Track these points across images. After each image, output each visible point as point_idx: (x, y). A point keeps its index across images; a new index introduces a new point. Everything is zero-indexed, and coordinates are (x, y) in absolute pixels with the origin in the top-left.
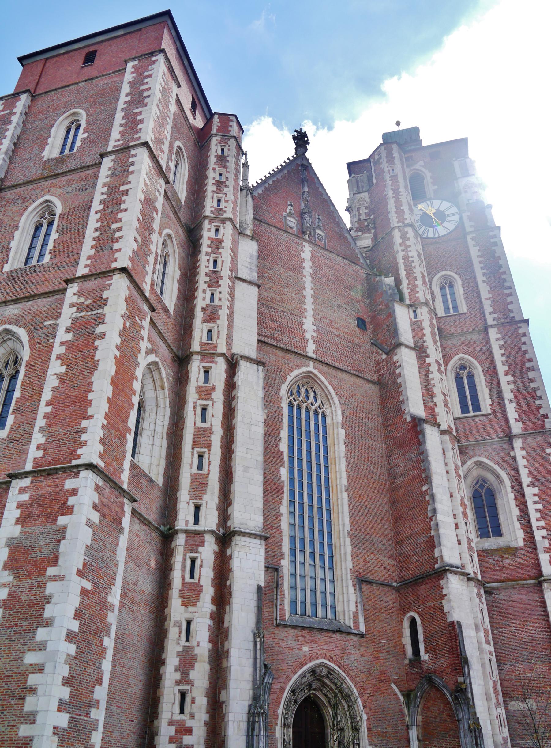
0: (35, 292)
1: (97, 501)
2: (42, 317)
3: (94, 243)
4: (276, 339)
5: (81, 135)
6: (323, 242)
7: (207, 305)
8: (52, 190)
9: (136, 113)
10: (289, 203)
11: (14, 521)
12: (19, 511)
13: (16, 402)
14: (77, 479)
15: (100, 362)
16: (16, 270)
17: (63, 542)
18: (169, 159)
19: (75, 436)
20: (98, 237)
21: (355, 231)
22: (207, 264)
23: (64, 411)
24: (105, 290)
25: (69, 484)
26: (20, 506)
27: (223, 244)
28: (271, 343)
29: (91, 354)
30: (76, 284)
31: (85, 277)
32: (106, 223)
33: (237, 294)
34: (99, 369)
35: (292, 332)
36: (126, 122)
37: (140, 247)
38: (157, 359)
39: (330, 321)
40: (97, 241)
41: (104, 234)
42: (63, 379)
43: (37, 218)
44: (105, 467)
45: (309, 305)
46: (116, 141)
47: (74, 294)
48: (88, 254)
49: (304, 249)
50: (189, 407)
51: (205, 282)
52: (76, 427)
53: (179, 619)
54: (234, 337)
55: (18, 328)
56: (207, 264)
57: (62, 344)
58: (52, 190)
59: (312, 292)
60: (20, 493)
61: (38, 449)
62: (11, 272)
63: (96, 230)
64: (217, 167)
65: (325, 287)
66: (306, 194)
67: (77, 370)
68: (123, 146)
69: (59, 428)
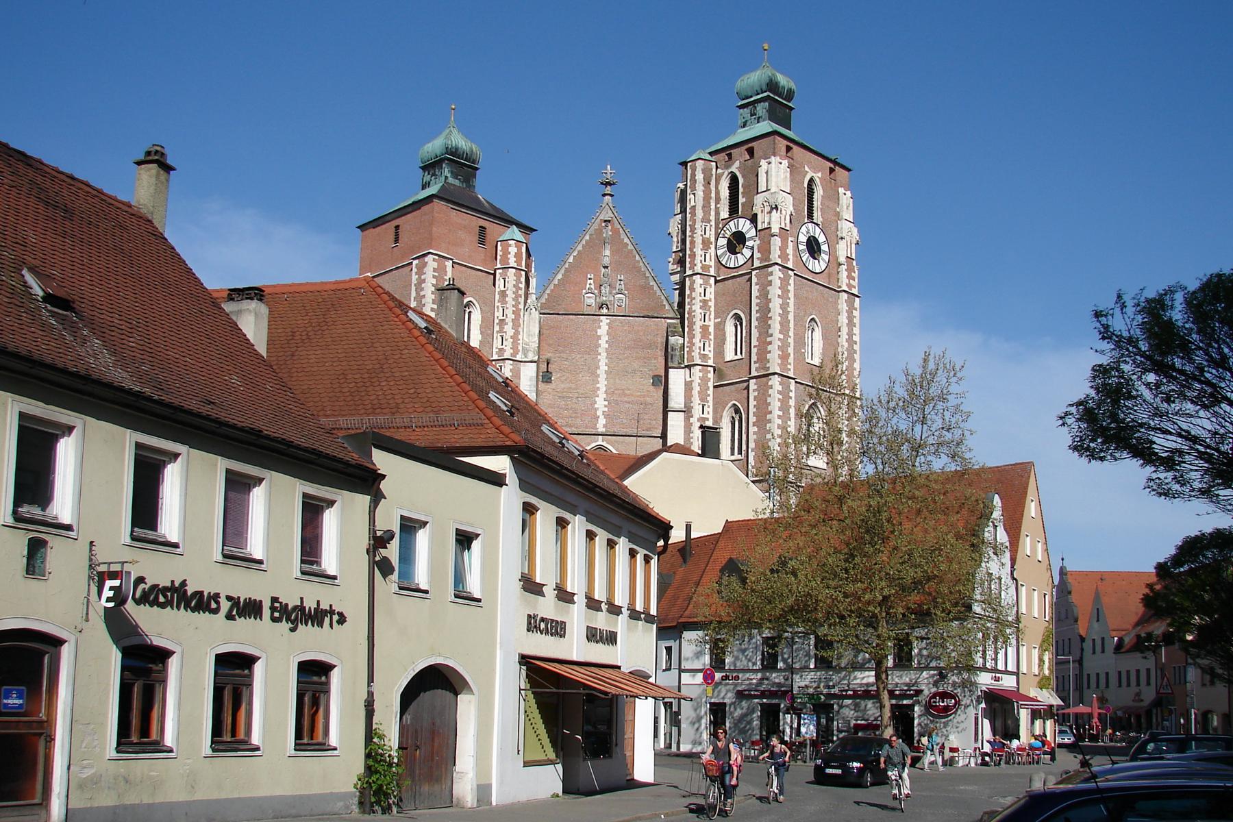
10: (589, 276)
21: (672, 264)
39: (623, 390)
45: (602, 384)
59: (606, 368)
64: (499, 304)
65: (620, 357)
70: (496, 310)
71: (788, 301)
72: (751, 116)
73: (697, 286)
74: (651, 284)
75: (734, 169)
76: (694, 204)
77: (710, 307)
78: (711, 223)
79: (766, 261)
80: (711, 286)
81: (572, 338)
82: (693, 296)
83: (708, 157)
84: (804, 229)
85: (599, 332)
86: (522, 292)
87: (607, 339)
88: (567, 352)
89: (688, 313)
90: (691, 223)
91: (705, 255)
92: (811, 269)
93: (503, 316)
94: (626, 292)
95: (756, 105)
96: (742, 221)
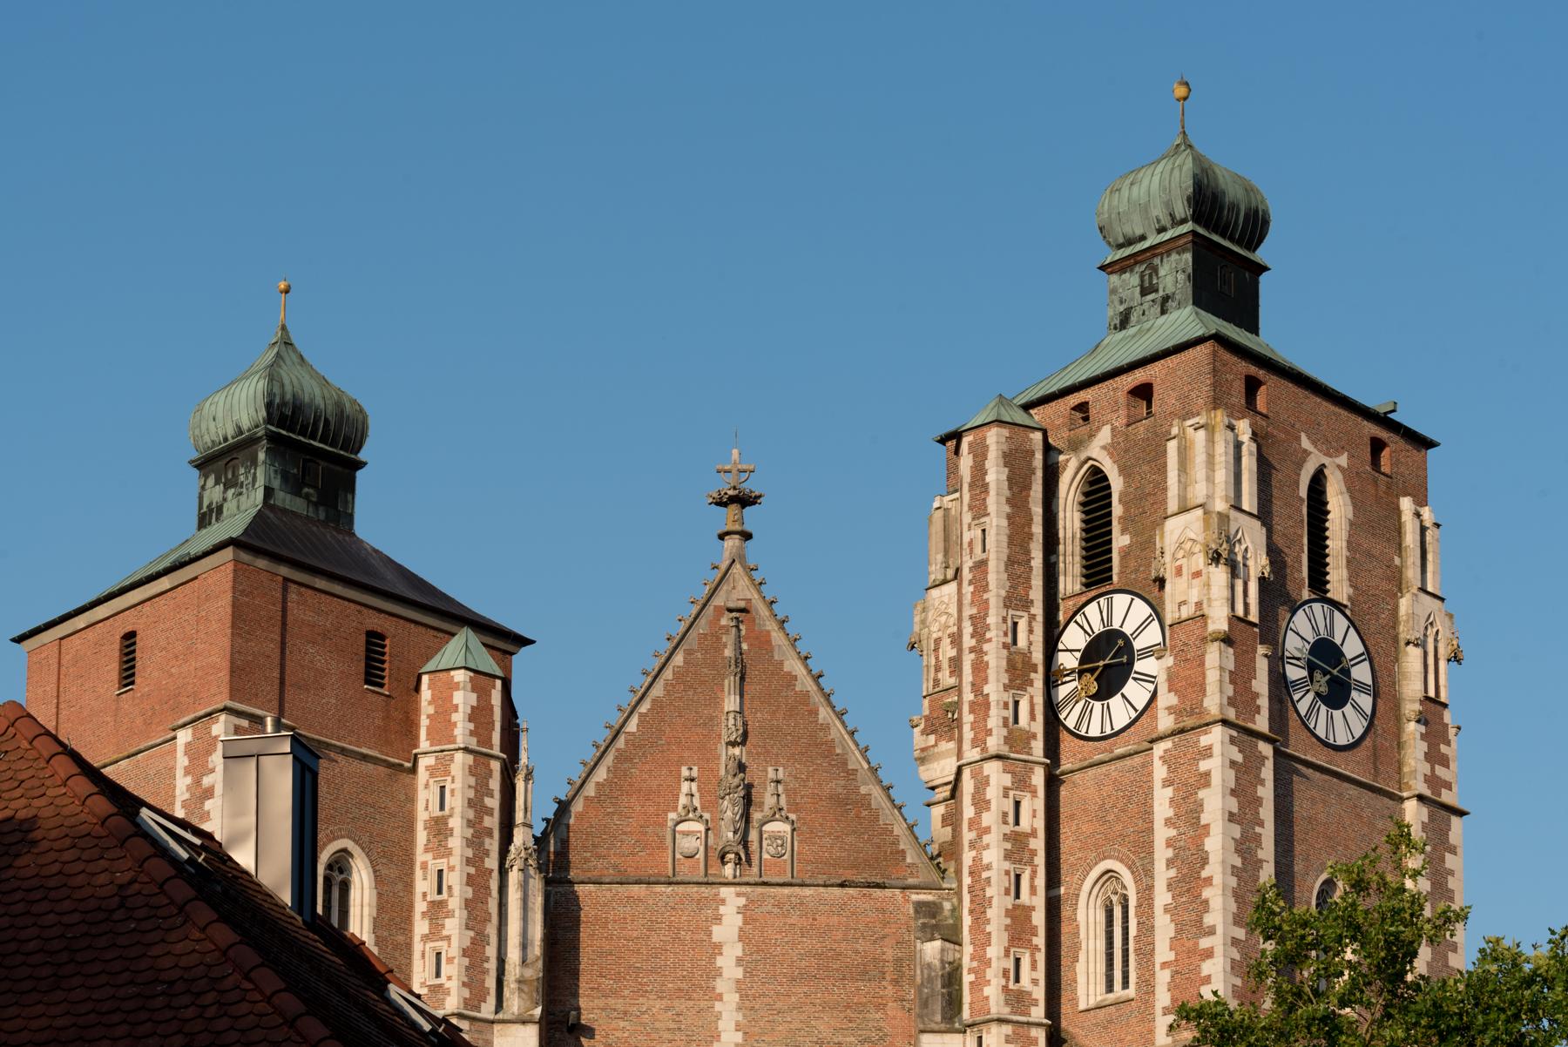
10: (685, 772)
65: (779, 1005)
70: (418, 873)
71: (1258, 829)
72: (1144, 292)
73: (992, 793)
74: (863, 790)
75: (1099, 449)
76: (984, 556)
77: (1034, 853)
78: (1033, 611)
79: (1191, 713)
80: (1034, 793)
81: (638, 952)
82: (984, 824)
83: (1020, 417)
84: (1300, 621)
85: (718, 933)
86: (493, 822)
87: (740, 953)
88: (626, 992)
89: (971, 873)
90: (974, 611)
91: (1016, 703)
92: (1322, 735)
93: (440, 892)
94: (793, 816)
95: (1157, 261)
96: (1121, 601)
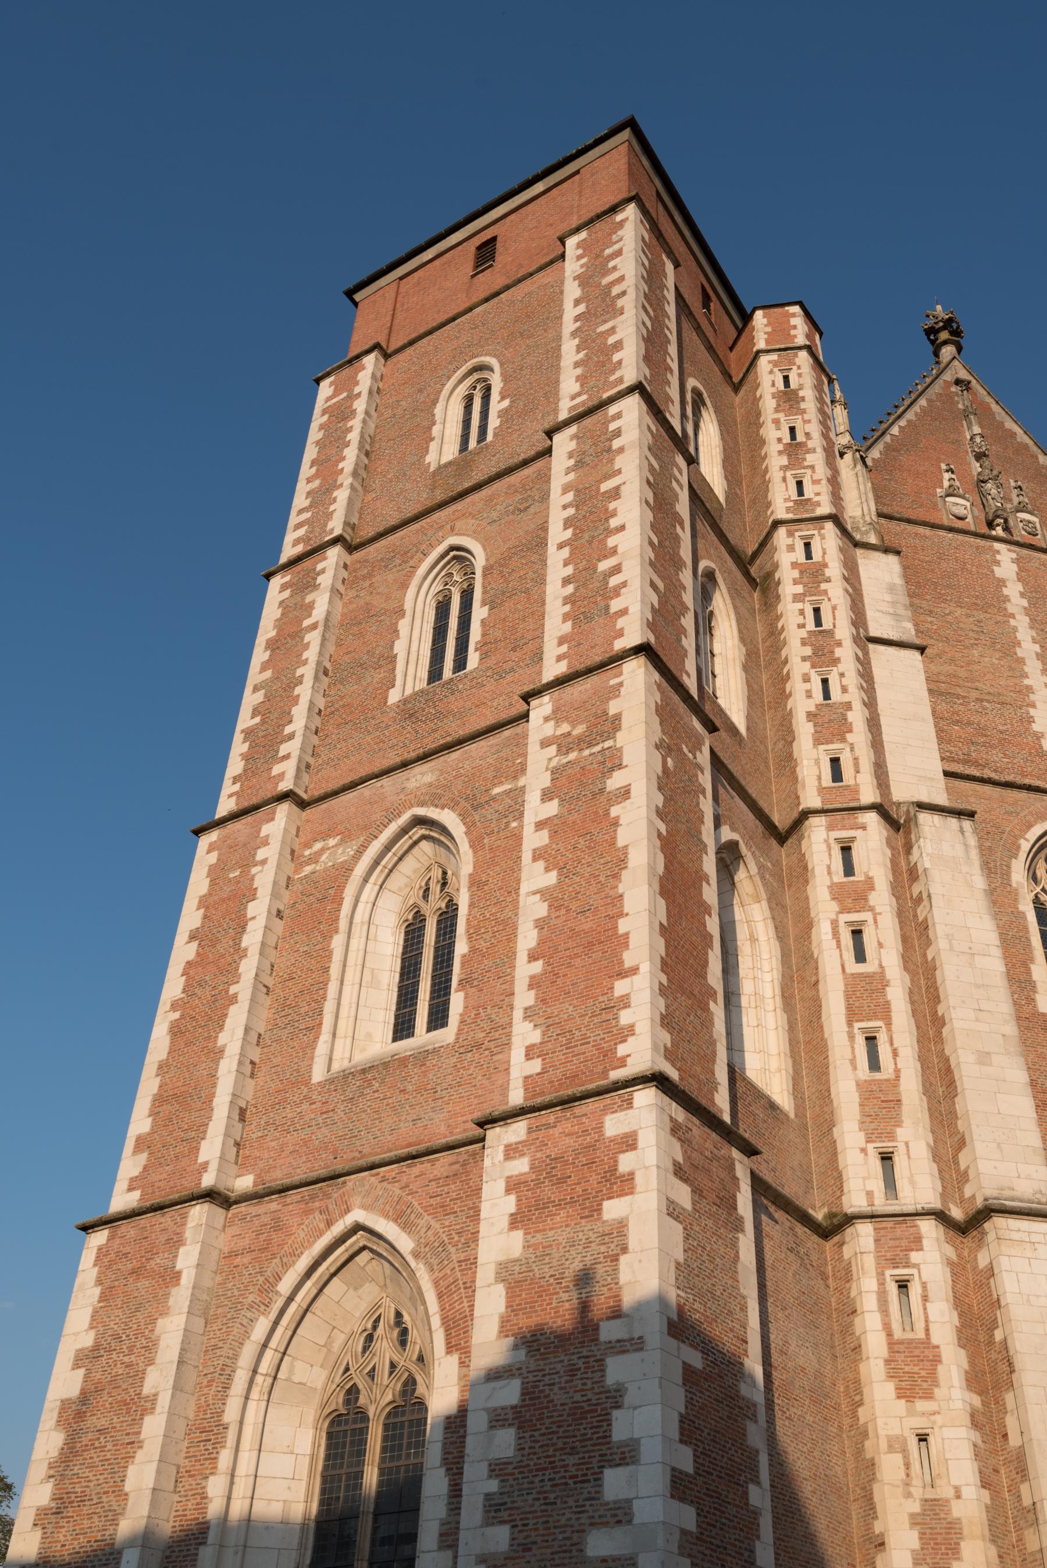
0: (461, 733)
1: (680, 1159)
2: (485, 779)
3: (567, 608)
4: (976, 764)
5: (497, 405)
6: (1039, 537)
7: (817, 706)
8: (458, 524)
9: (602, 333)
10: (944, 467)
11: (505, 1222)
12: (512, 1199)
13: (463, 964)
14: (630, 1112)
15: (630, 850)
16: (416, 695)
17: (623, 1259)
18: (684, 416)
19: (604, 1017)
20: (573, 594)
22: (801, 620)
23: (570, 965)
24: (610, 699)
25: (614, 1125)
26: (513, 1186)
27: (828, 572)
28: (967, 772)
29: (606, 837)
30: (546, 699)
31: (560, 682)
32: (584, 563)
33: (877, 672)
34: (630, 865)
35: (1009, 742)
36: (586, 355)
37: (663, 599)
38: (735, 836)
40: (573, 603)
41: (585, 585)
42: (556, 899)
43: (438, 587)
44: (681, 1079)
46: (573, 398)
47: (547, 719)
48: (560, 634)
49: (998, 557)
50: (823, 931)
51: (804, 659)
52: (605, 998)
53: (897, 1431)
54: (891, 767)
55: (438, 810)
56: (801, 620)
57: (540, 825)
58: (458, 524)
59: (1037, 648)
60: (508, 1157)
61: (528, 1057)
62: (405, 701)
63: (566, 581)
64: (781, 416)
66: (978, 439)
67: (582, 876)
68: (590, 404)
69: (567, 1005)
88: (928, 597)
